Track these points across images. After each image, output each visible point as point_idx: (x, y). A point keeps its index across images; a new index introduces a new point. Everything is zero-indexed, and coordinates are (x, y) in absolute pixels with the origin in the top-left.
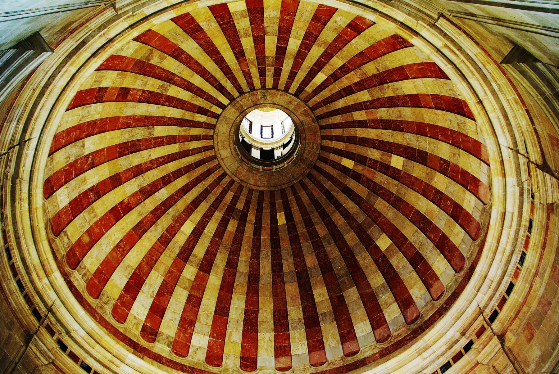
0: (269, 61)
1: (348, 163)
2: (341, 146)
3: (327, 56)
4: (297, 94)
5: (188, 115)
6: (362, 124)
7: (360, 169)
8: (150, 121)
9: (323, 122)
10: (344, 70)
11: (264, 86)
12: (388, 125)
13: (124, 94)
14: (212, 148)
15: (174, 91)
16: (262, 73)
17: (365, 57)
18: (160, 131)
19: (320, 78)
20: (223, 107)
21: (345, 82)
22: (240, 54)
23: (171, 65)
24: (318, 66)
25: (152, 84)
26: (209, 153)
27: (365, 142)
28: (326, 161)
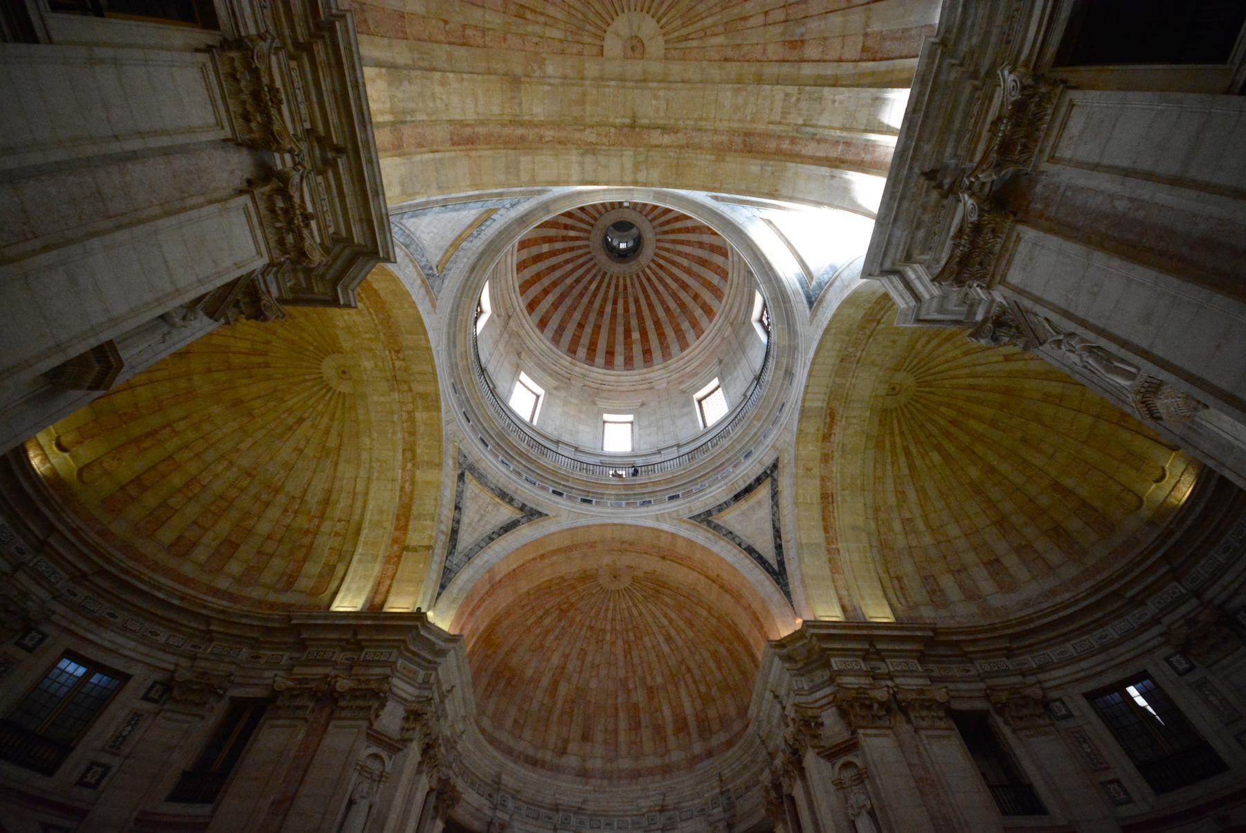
0: (621, 296)
1: (572, 233)
2: (577, 243)
3: (591, 303)
4: (605, 273)
5: (668, 266)
6: (567, 262)
7: (564, 233)
8: (689, 272)
9: (589, 256)
10: (581, 295)
11: (624, 279)
12: (553, 268)
13: (696, 297)
14: (658, 241)
15: (674, 285)
16: (625, 286)
17: (573, 308)
18: (685, 262)
19: (593, 287)
20: (649, 267)
21: (579, 287)
22: (637, 301)
23: (672, 305)
24: (595, 295)
25: (683, 295)
26: (661, 237)
27: (564, 251)
28: (586, 231)
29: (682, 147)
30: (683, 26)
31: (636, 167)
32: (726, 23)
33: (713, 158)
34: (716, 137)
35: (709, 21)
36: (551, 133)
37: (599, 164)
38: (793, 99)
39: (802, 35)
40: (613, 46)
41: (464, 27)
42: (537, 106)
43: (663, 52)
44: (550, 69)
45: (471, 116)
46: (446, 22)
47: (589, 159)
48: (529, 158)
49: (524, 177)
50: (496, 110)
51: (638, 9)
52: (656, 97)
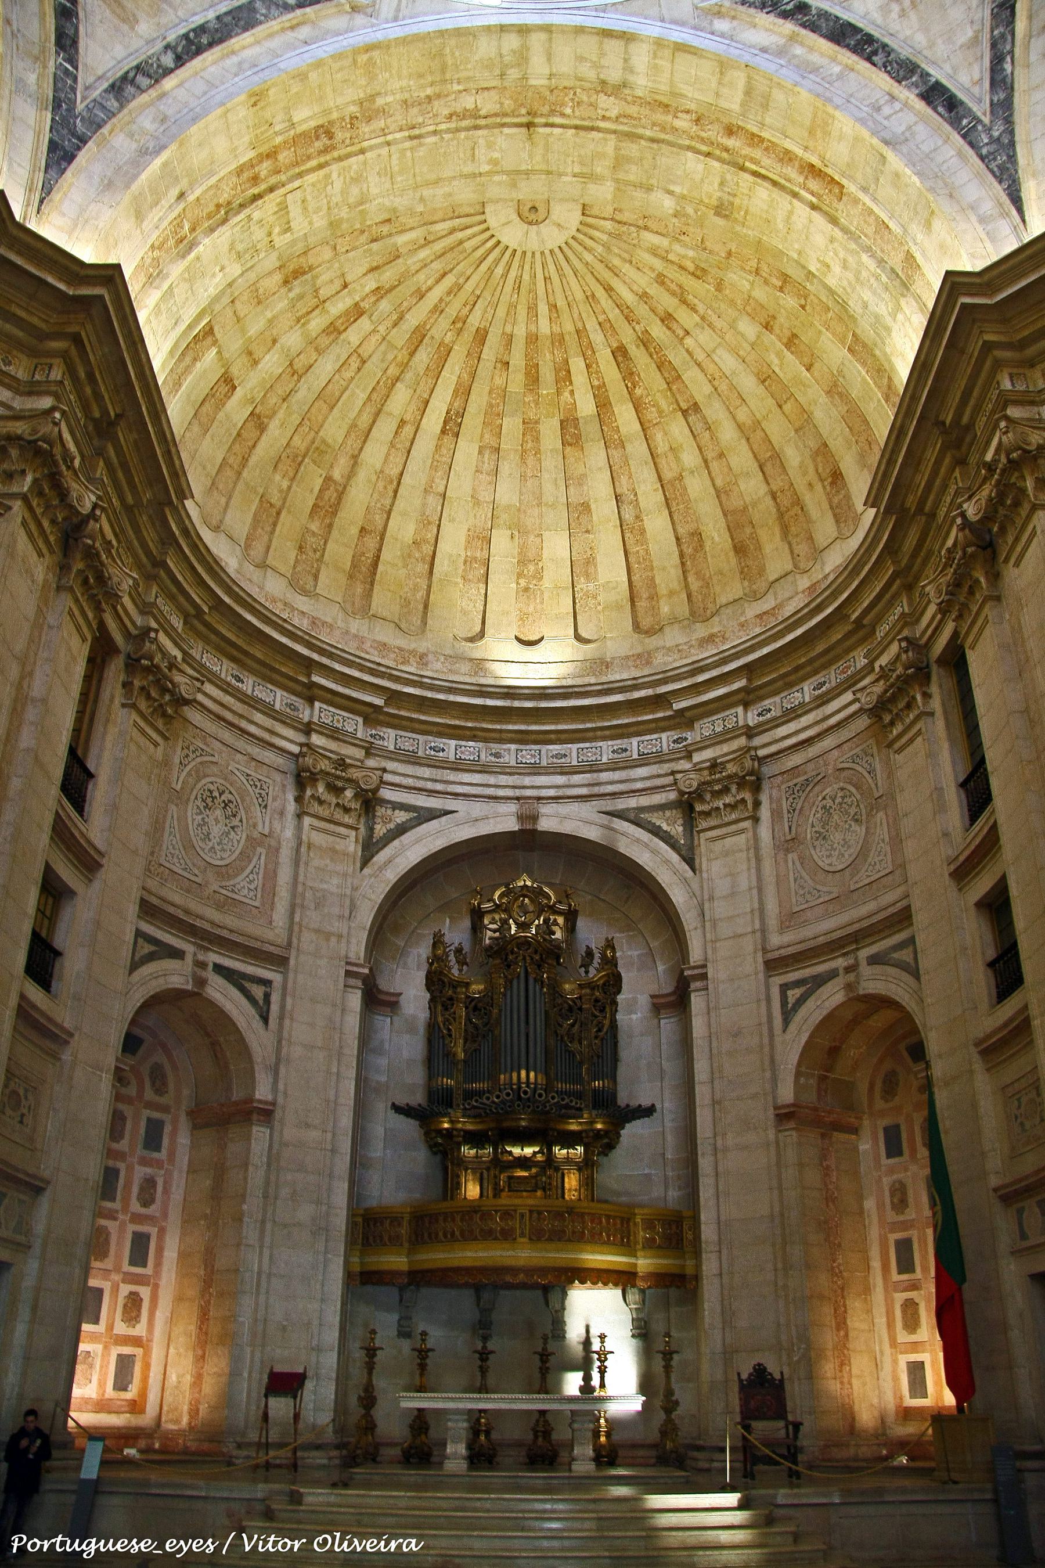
29: (439, 96)
30: (461, 242)
31: (522, 57)
32: (398, 257)
33: (380, 101)
34: (382, 124)
35: (423, 254)
36: (678, 123)
37: (596, 66)
38: (277, 230)
39: (290, 290)
40: (568, 216)
41: (781, 289)
42: (697, 174)
43: (488, 209)
44: (668, 204)
45: (802, 211)
46: (803, 307)
47: (614, 76)
48: (724, 104)
49: (739, 78)
50: (763, 192)
51: (529, 255)
52: (495, 162)
